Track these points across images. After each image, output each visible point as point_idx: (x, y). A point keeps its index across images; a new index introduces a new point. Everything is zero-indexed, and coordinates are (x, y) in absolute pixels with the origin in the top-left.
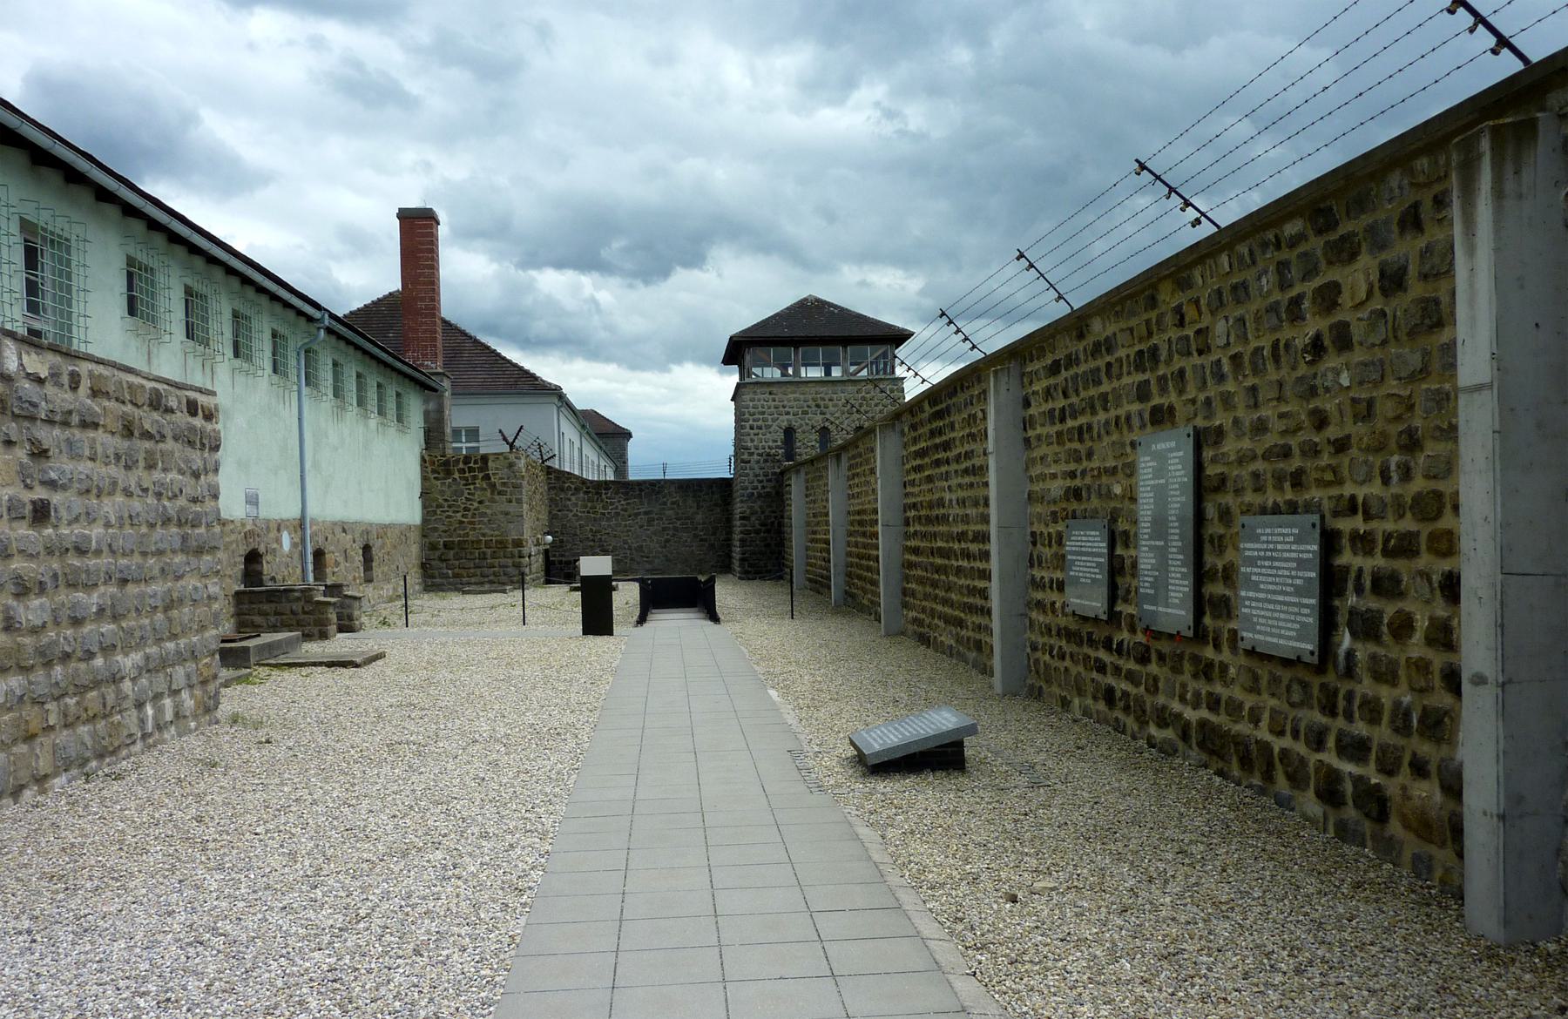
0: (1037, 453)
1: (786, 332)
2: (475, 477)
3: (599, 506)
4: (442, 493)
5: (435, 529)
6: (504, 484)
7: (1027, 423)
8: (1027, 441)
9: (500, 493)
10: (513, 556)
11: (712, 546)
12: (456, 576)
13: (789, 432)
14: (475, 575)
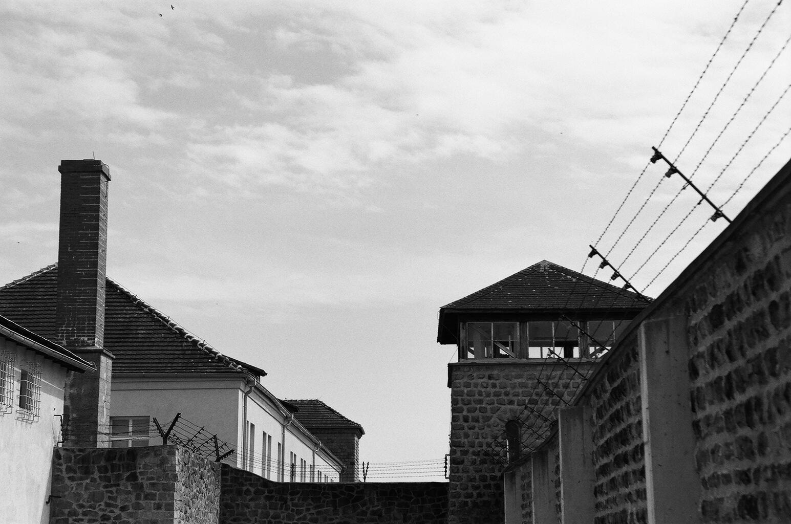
0: (709, 444)
1: (510, 304)
7: (696, 400)
8: (696, 425)
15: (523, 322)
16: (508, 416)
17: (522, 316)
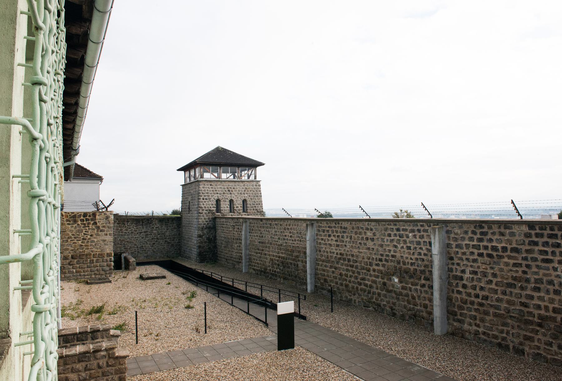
1: (211, 161)
2: (89, 224)
3: (124, 229)
4: (71, 231)
5: (68, 249)
6: (104, 226)
9: (101, 231)
10: (107, 261)
11: (173, 245)
12: (76, 272)
13: (218, 201)
14: (87, 271)
15: (220, 167)
16: (216, 198)
17: (220, 165)
